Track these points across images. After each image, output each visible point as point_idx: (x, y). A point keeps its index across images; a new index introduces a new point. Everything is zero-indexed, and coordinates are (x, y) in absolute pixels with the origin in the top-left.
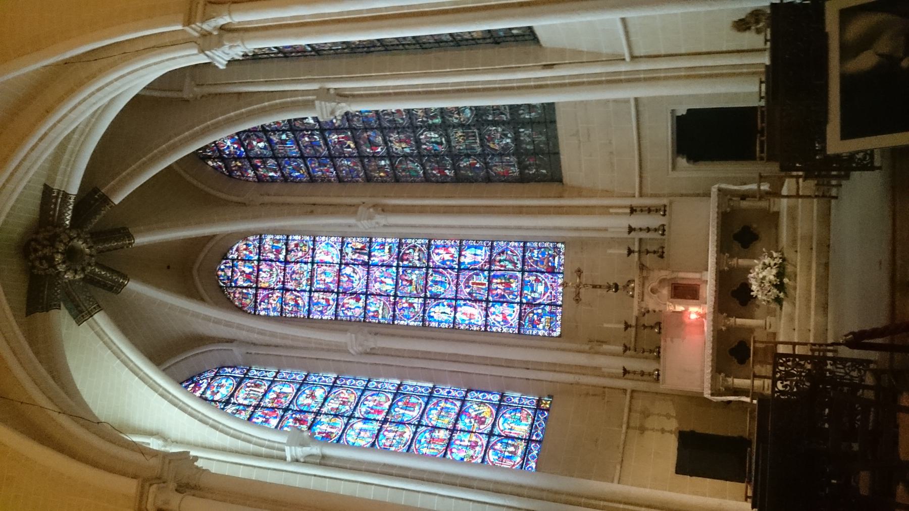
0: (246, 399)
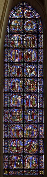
0: (26, 41)
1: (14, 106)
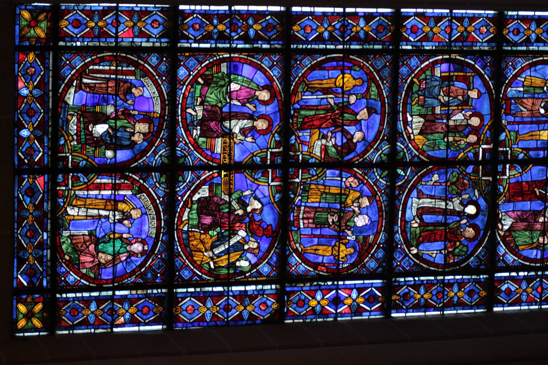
1: (512, 92)
